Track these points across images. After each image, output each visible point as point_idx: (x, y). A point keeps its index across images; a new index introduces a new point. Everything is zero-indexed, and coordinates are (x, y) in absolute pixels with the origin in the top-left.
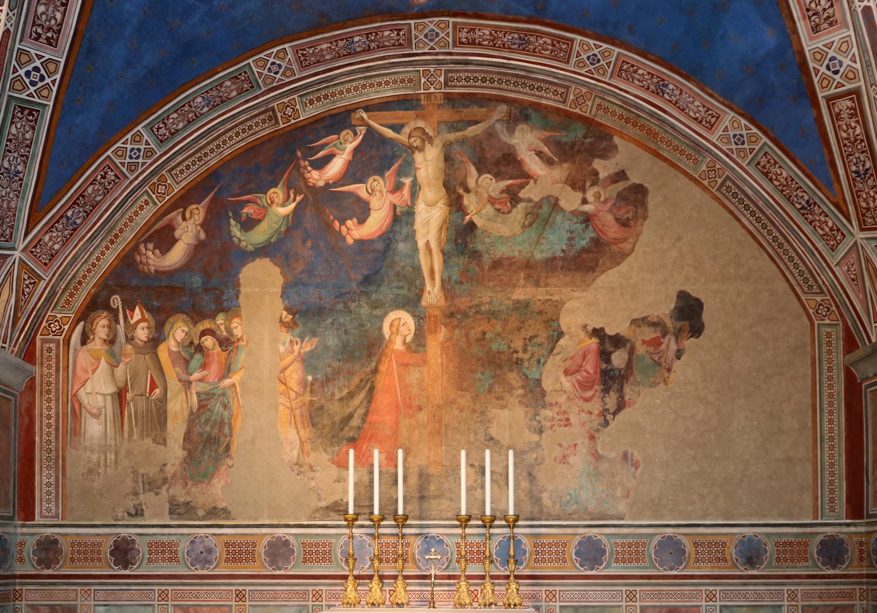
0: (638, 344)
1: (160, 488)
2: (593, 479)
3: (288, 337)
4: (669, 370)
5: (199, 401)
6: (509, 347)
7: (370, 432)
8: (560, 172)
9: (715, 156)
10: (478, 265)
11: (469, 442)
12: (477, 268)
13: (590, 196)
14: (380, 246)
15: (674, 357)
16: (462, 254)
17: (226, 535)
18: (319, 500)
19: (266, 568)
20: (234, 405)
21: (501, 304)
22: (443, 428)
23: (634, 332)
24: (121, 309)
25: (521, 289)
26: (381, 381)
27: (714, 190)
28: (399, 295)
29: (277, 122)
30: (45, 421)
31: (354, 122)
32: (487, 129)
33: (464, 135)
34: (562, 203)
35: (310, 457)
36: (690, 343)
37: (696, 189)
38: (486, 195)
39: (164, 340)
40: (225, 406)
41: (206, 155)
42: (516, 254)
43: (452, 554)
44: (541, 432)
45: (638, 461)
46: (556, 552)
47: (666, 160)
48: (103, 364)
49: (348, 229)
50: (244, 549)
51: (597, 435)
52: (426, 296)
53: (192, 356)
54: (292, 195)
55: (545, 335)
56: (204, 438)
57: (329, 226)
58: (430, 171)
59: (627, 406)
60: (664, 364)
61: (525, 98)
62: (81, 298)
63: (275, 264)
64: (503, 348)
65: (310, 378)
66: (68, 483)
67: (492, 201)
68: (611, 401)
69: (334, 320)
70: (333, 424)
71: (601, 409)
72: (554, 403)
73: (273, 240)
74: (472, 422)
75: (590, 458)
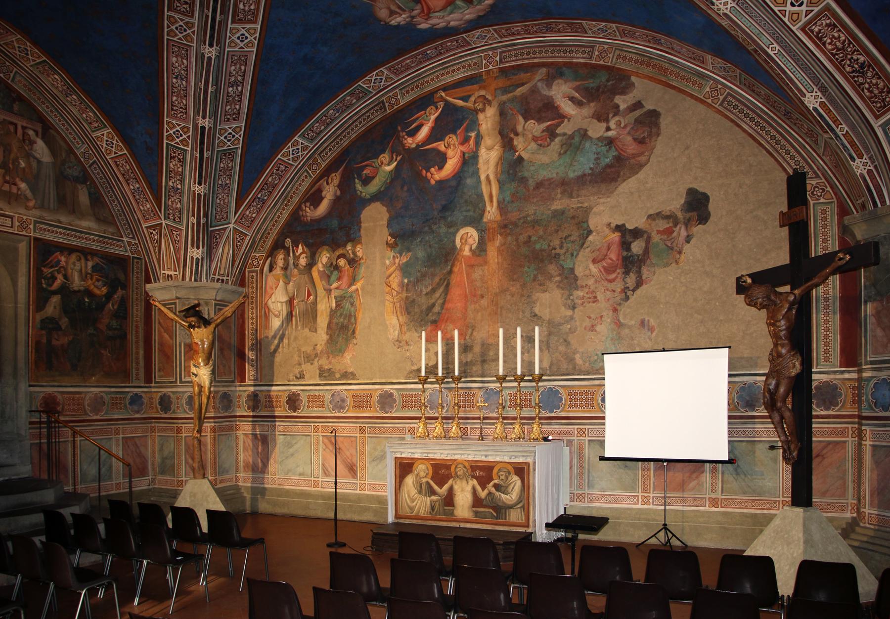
0: (654, 234)
1: (313, 360)
2: (616, 342)
3: (391, 254)
4: (680, 253)
5: (336, 302)
6: (549, 246)
7: (446, 316)
8: (587, 111)
9: (714, 79)
10: (525, 188)
11: (518, 319)
12: (524, 190)
13: (612, 124)
14: (453, 183)
15: (684, 242)
16: (513, 181)
17: (353, 390)
18: (413, 365)
19: (378, 412)
20: (357, 303)
21: (542, 215)
22: (499, 310)
23: (650, 225)
24: (291, 247)
25: (558, 201)
26: (454, 279)
27: (716, 106)
28: (467, 216)
29: (385, 110)
30: (251, 321)
31: (435, 100)
32: (531, 88)
33: (514, 95)
34: (590, 133)
35: (406, 335)
36: (698, 229)
37: (701, 107)
38: (530, 136)
39: (316, 264)
40: (352, 304)
41: (341, 140)
42: (554, 175)
43: (506, 402)
44: (574, 308)
45: (653, 327)
46: (586, 399)
47: (674, 88)
48: (281, 283)
49: (432, 174)
50: (364, 399)
51: (619, 308)
52: (487, 214)
53: (332, 273)
54: (394, 157)
55: (577, 234)
56: (339, 327)
57: (418, 174)
58: (489, 125)
59: (644, 284)
60: (675, 248)
61: (560, 60)
62: (269, 243)
63: (384, 205)
64: (545, 246)
65: (406, 281)
66: (263, 358)
67: (535, 139)
68: (631, 280)
69: (422, 239)
70: (421, 311)
71: (623, 287)
72: (585, 285)
73: (382, 190)
74: (521, 304)
75: (613, 326)
